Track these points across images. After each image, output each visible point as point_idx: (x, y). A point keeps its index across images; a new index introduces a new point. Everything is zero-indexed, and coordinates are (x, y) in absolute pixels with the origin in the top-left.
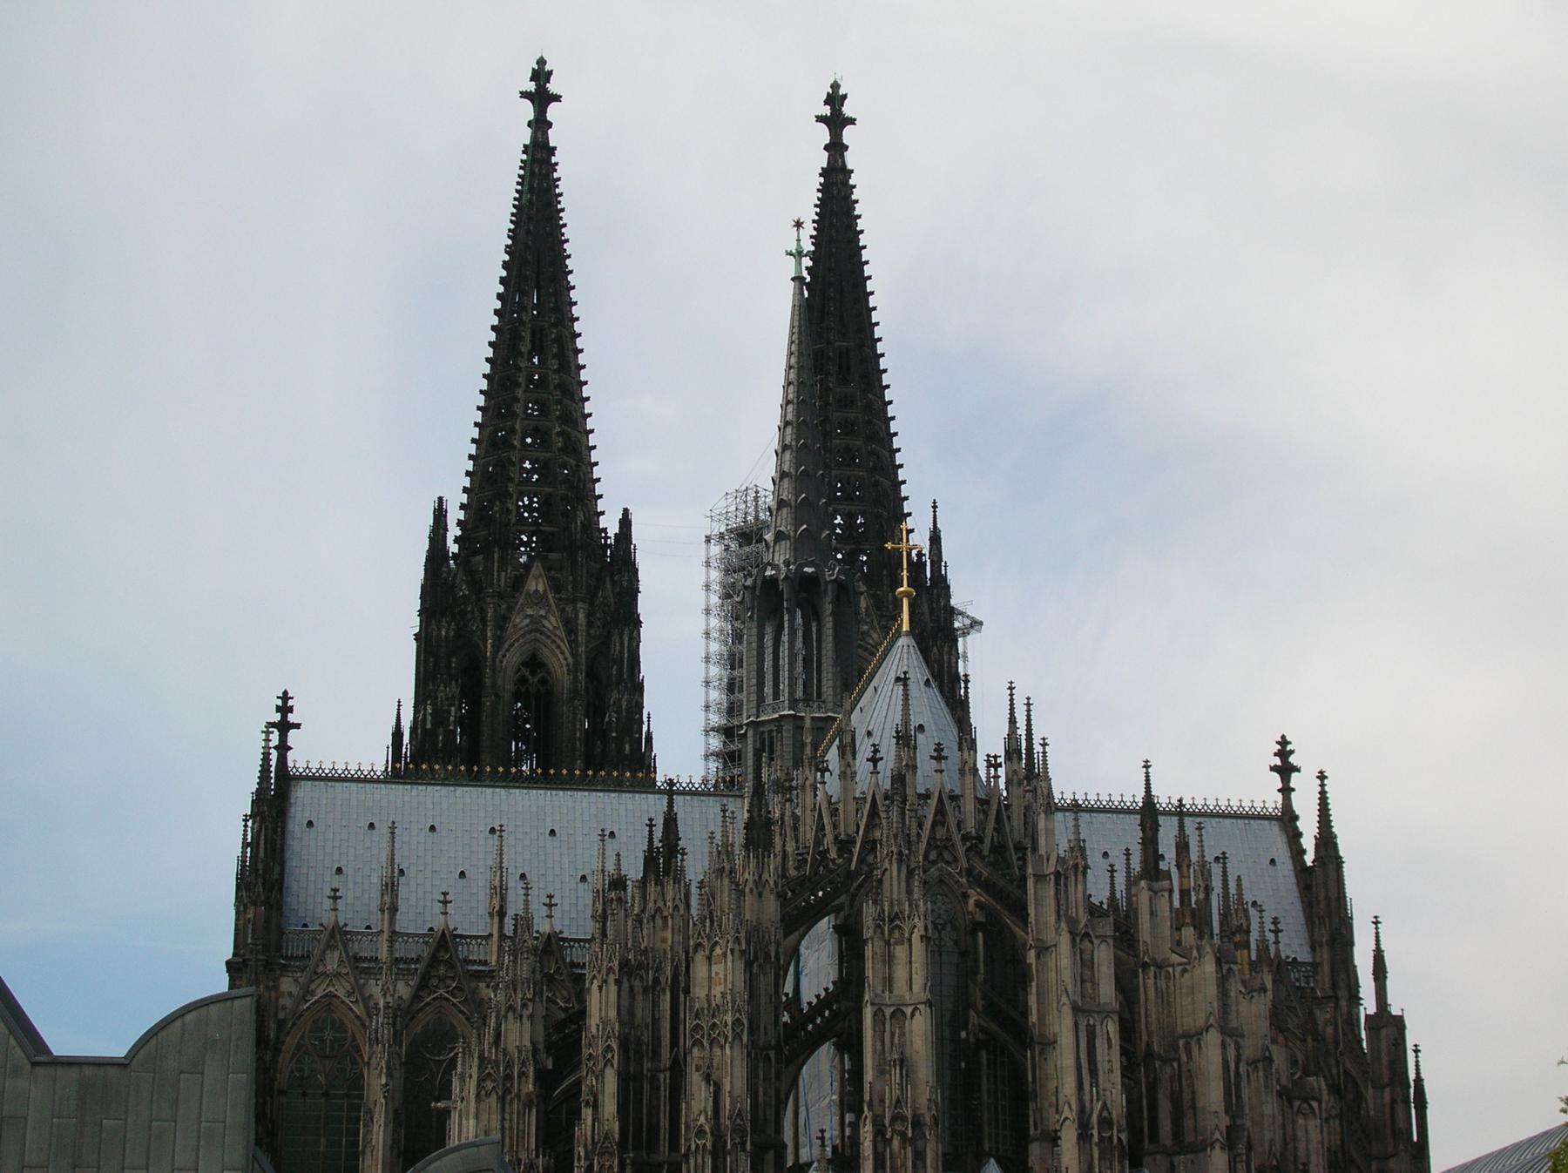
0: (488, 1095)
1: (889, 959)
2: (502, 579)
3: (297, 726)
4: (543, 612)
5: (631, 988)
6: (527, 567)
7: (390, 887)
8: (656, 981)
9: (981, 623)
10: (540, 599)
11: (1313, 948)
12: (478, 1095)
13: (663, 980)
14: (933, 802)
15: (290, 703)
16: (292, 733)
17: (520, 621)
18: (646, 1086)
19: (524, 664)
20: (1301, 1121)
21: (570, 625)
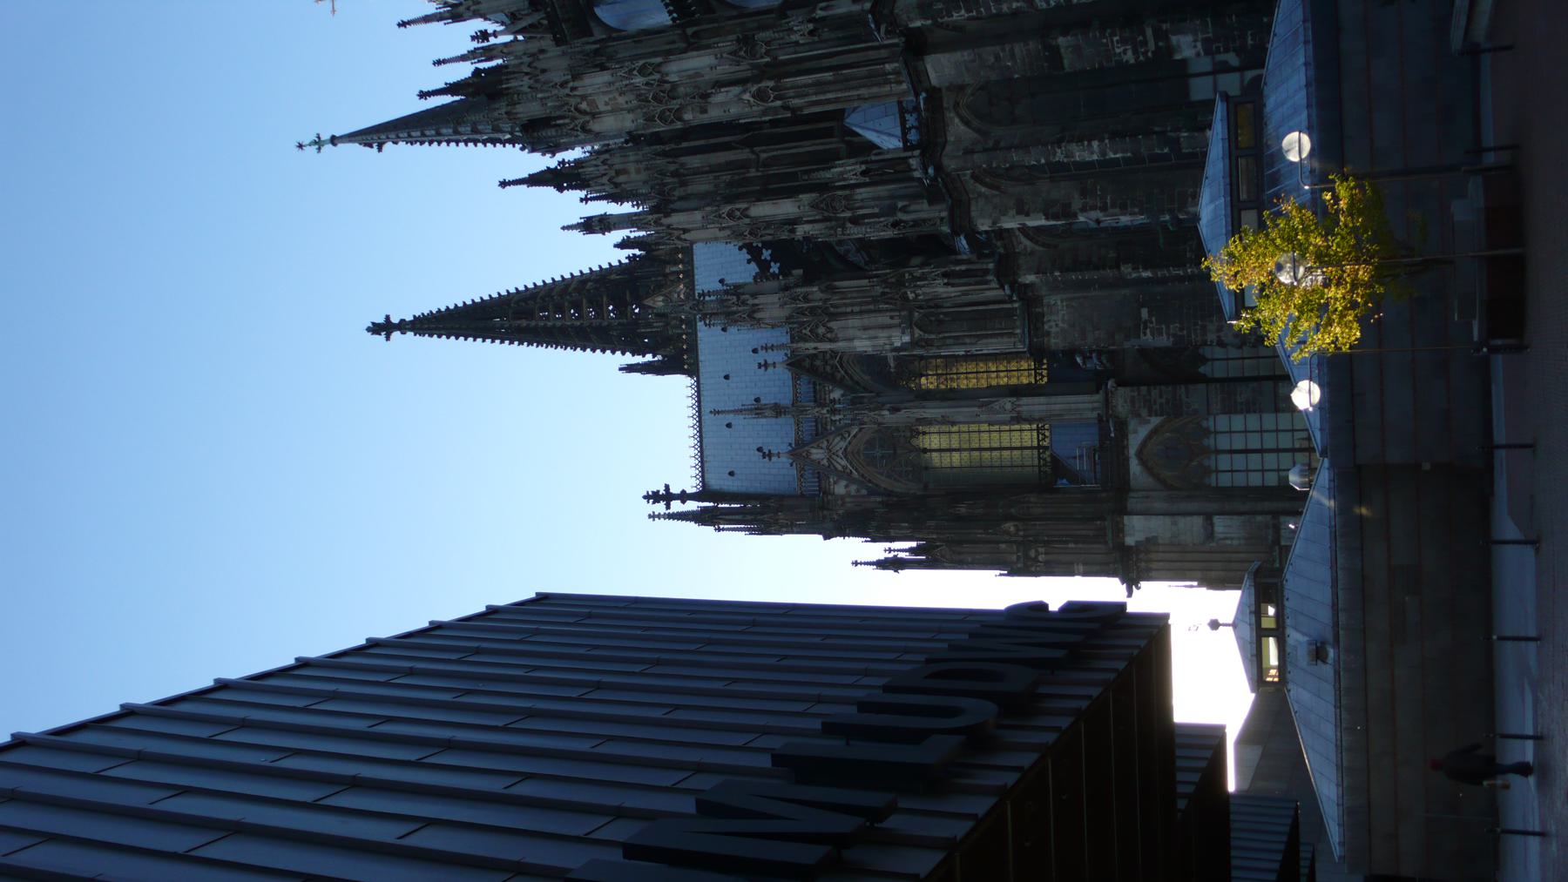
0: (830, 330)
3: (667, 487)
5: (681, 198)
8: (674, 174)
12: (831, 341)
13: (672, 168)
16: (672, 490)
18: (774, 171)
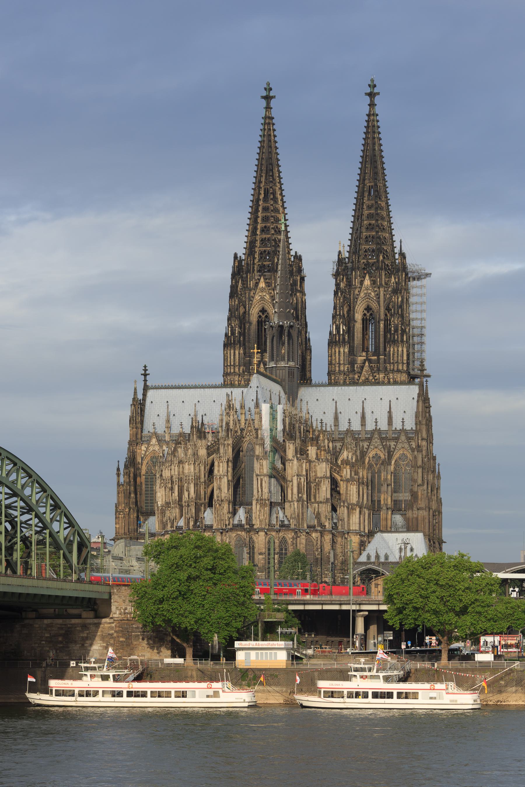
1: (219, 466)
2: (252, 284)
3: (149, 374)
4: (264, 294)
6: (259, 280)
7: (168, 421)
9: (431, 274)
10: (262, 290)
11: (416, 424)
14: (248, 422)
15: (147, 368)
16: (148, 376)
17: (257, 297)
19: (260, 311)
20: (352, 487)
21: (273, 298)
